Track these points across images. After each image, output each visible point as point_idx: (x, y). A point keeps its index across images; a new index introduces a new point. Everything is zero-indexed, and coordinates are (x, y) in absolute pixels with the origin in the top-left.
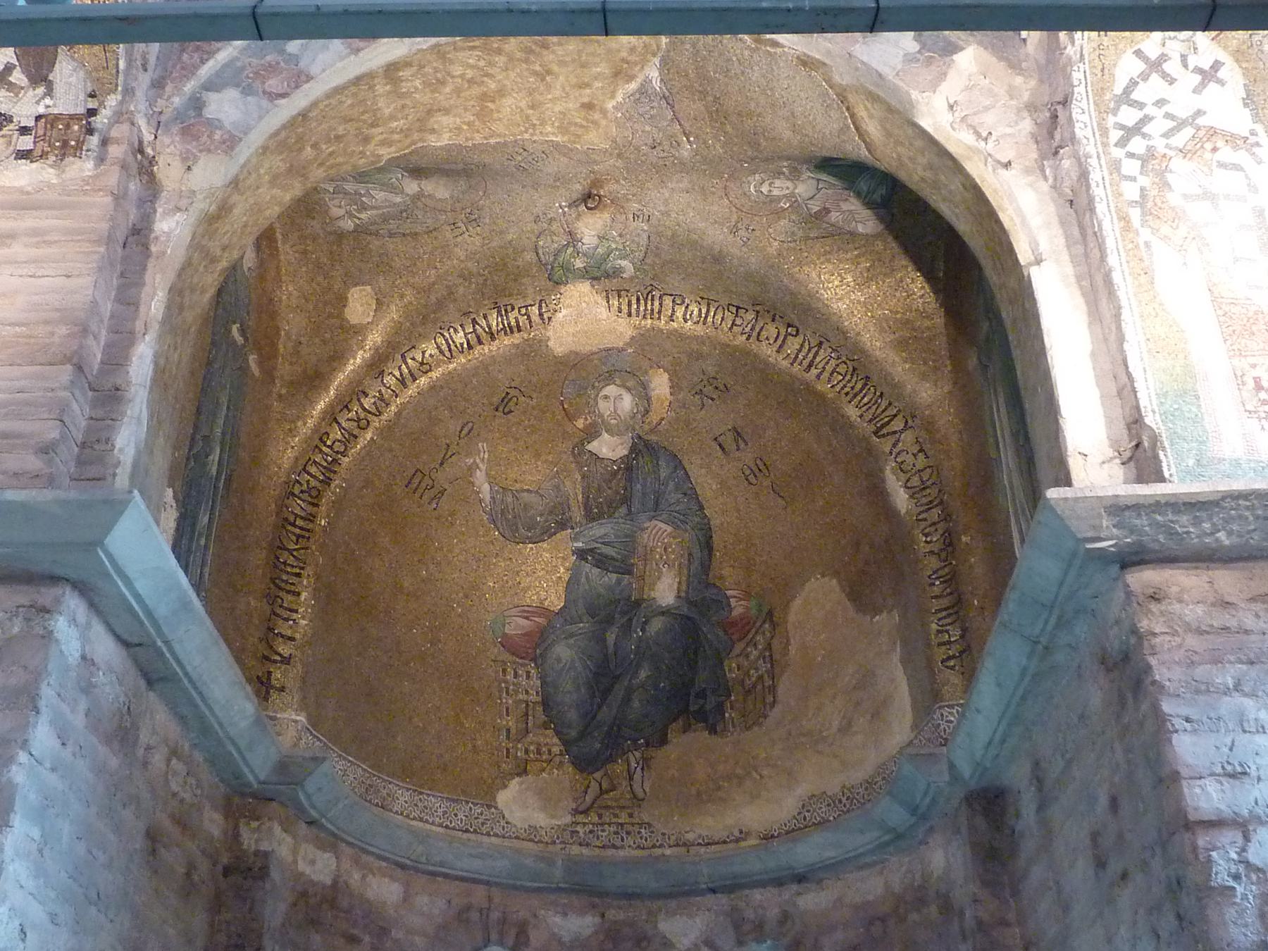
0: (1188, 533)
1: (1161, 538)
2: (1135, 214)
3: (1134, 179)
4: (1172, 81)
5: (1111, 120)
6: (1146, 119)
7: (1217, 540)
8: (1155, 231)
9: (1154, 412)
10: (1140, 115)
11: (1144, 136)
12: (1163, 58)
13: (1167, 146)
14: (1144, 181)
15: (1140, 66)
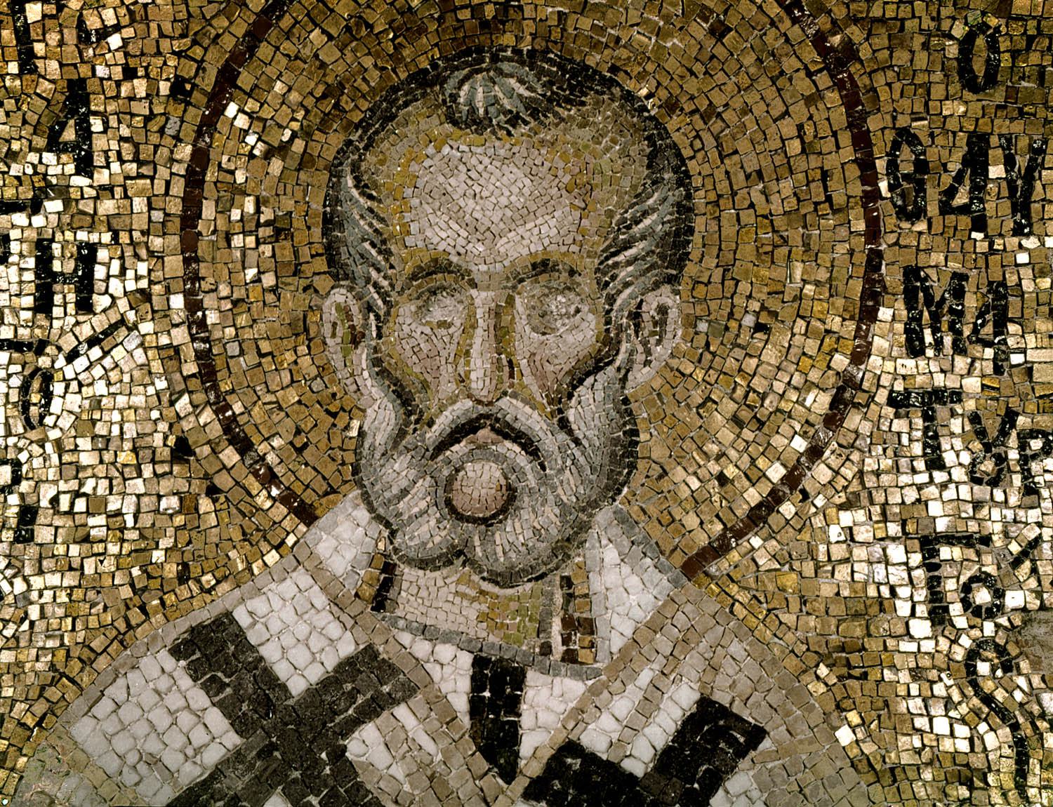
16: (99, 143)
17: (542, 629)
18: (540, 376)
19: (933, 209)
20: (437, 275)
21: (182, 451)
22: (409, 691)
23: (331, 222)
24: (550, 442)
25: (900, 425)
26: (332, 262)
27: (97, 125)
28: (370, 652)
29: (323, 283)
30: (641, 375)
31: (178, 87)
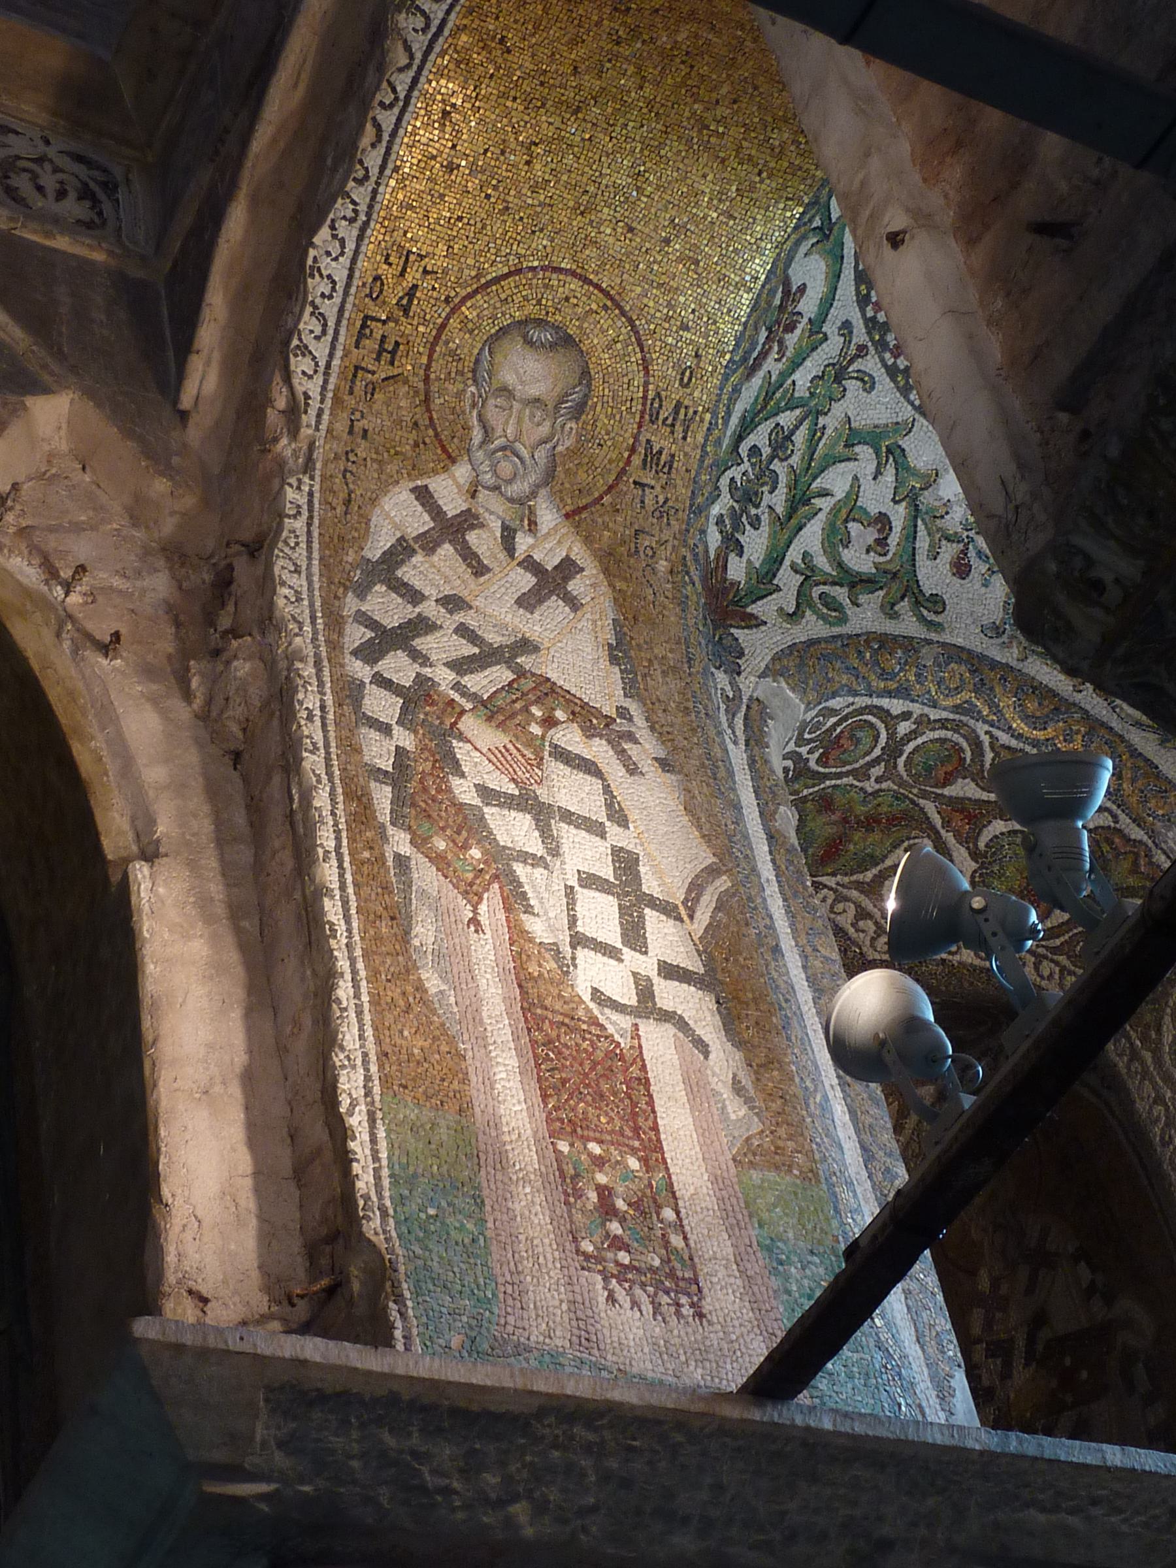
0: (447, 1491)
1: (384, 1495)
2: (383, 797)
3: (386, 730)
4: (479, 569)
5: (351, 604)
6: (422, 626)
7: (509, 1522)
8: (419, 842)
9: (384, 1214)
10: (411, 612)
11: (416, 656)
12: (468, 520)
13: (457, 686)
14: (405, 739)
15: (419, 522)
16: (413, 308)
17: (522, 520)
18: (529, 438)
19: (660, 423)
20: (506, 391)
21: (416, 424)
22: (482, 526)
23: (477, 361)
24: (528, 461)
25: (635, 491)
26: (474, 376)
27: (416, 302)
28: (469, 510)
29: (470, 382)
30: (560, 448)
31: (447, 297)
